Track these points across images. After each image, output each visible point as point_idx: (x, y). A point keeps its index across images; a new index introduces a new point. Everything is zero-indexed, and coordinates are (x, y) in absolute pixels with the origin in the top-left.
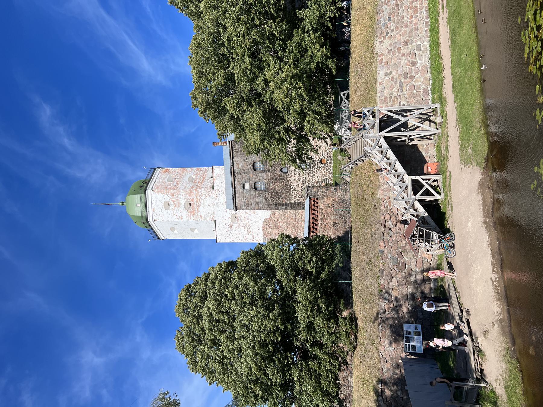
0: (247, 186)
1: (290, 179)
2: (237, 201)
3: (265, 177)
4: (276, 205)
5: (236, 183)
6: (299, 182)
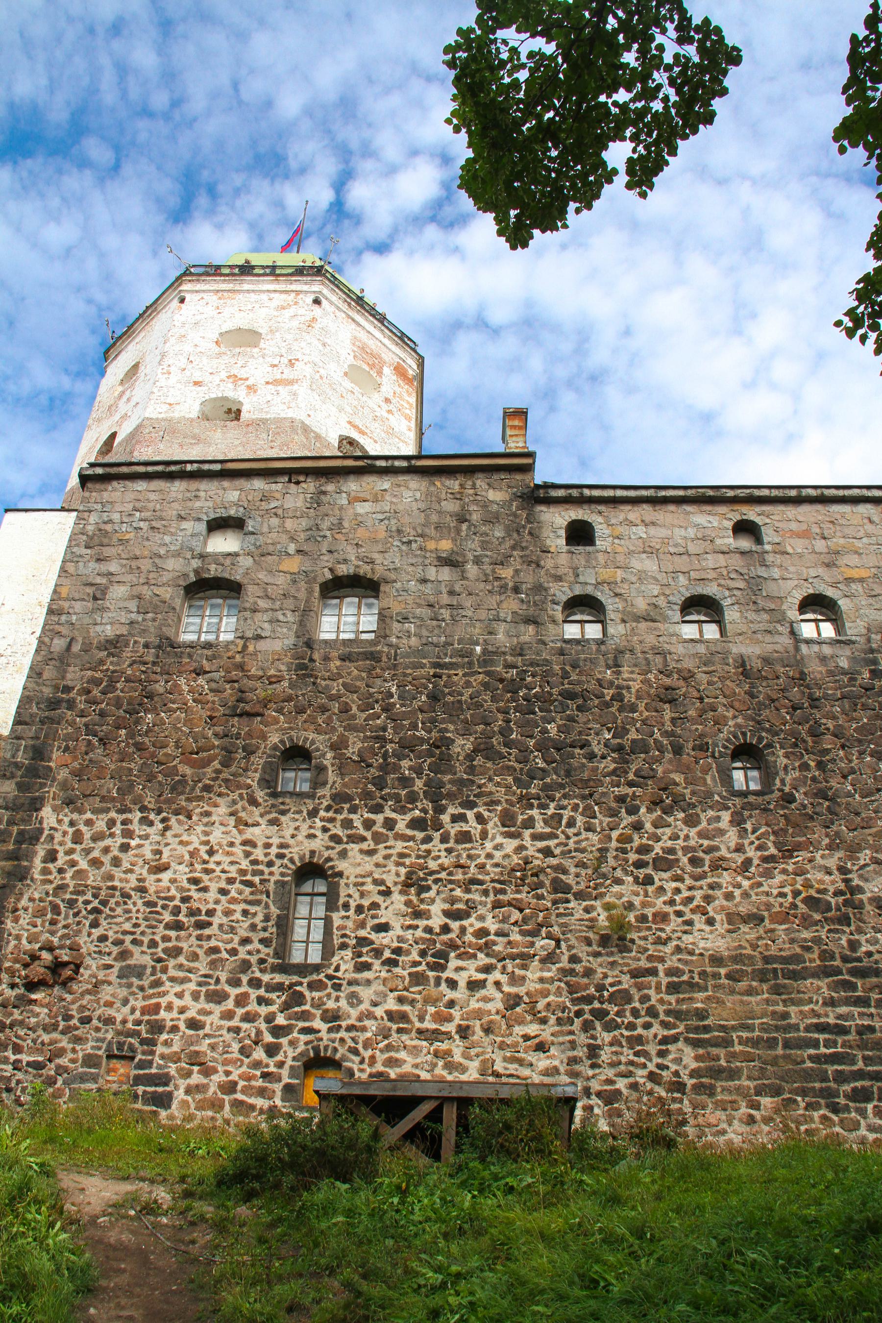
0: (223, 543)
1: (221, 810)
2: (141, 485)
3: (262, 645)
4: (53, 704)
5: (258, 484)
6: (182, 872)
